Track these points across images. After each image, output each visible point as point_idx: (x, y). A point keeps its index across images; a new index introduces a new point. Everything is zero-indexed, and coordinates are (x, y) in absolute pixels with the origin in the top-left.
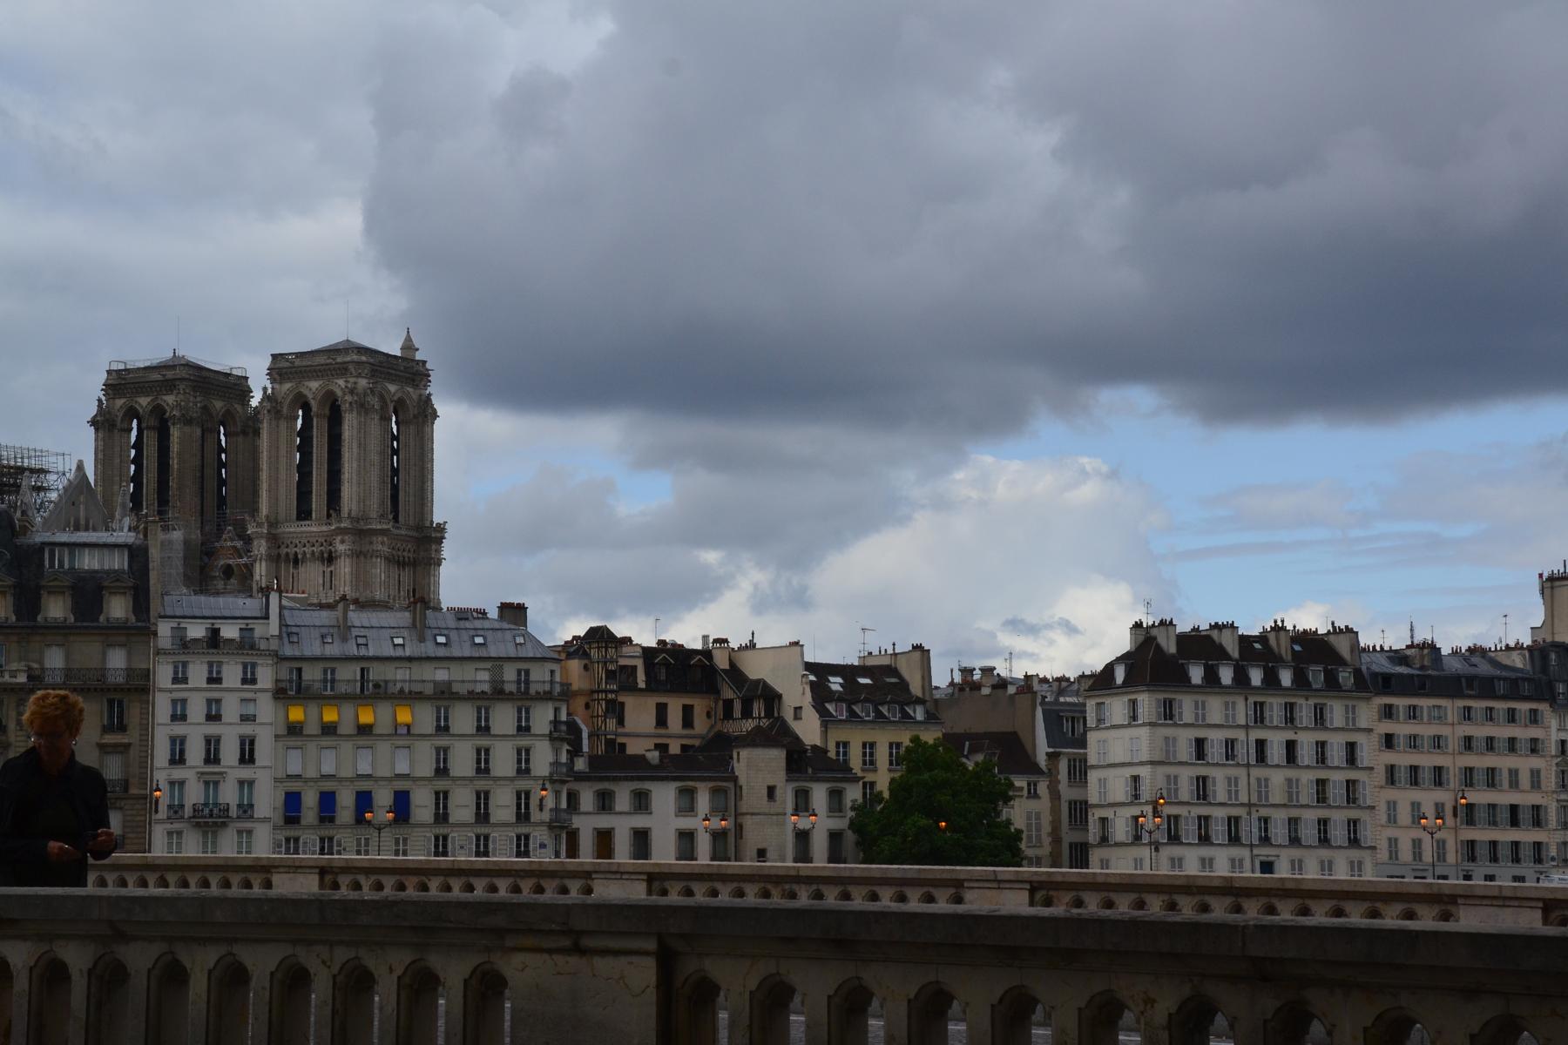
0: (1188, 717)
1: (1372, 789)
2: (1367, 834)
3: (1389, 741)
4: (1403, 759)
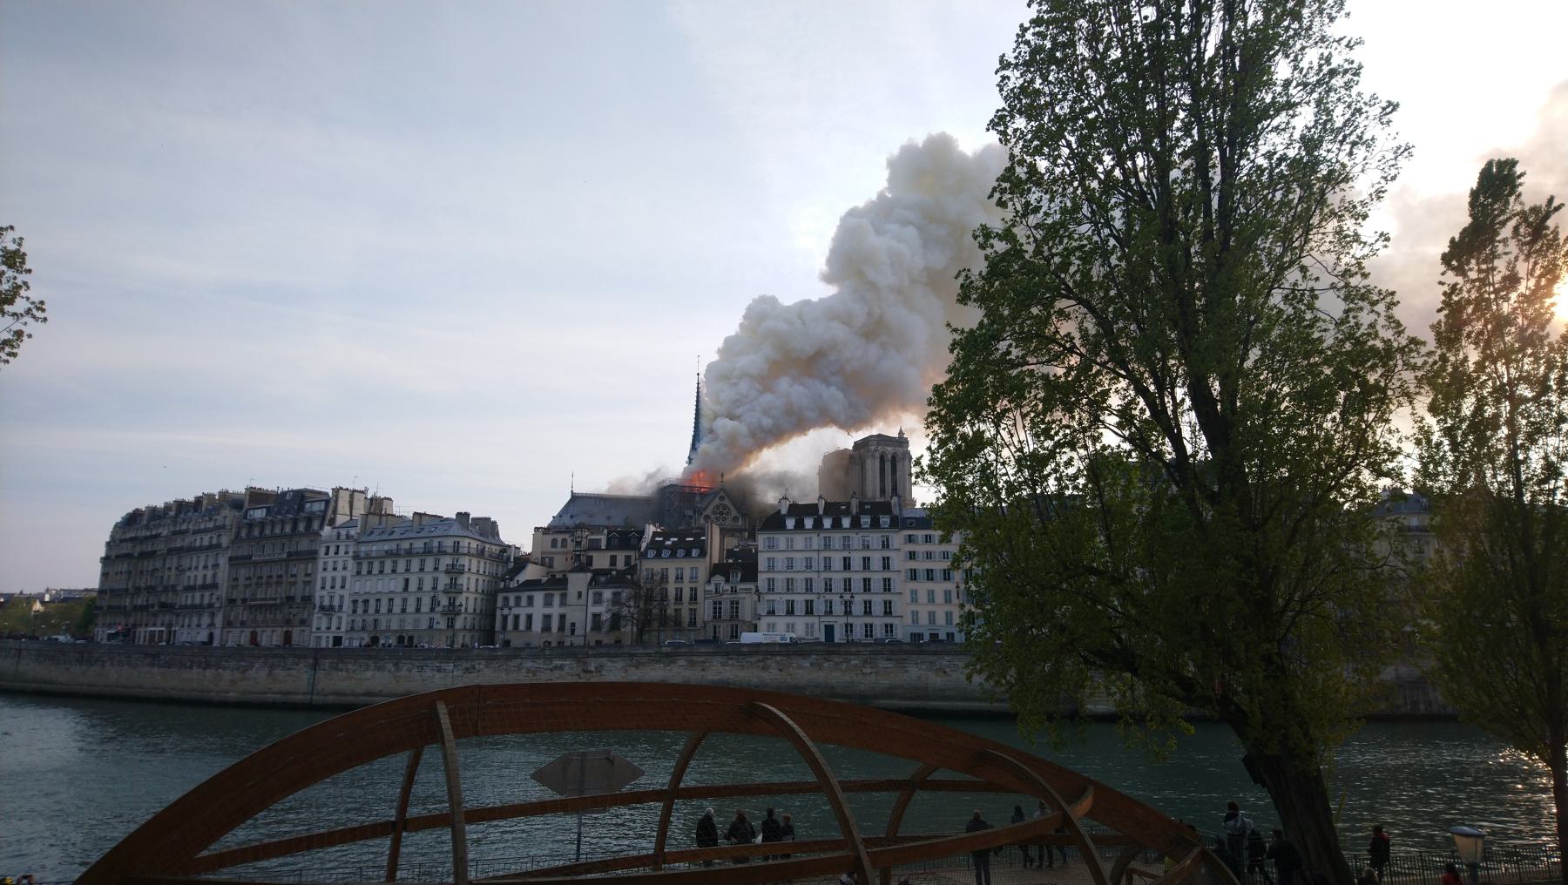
0: (782, 546)
1: (899, 582)
2: (896, 609)
3: (912, 556)
4: (921, 565)
